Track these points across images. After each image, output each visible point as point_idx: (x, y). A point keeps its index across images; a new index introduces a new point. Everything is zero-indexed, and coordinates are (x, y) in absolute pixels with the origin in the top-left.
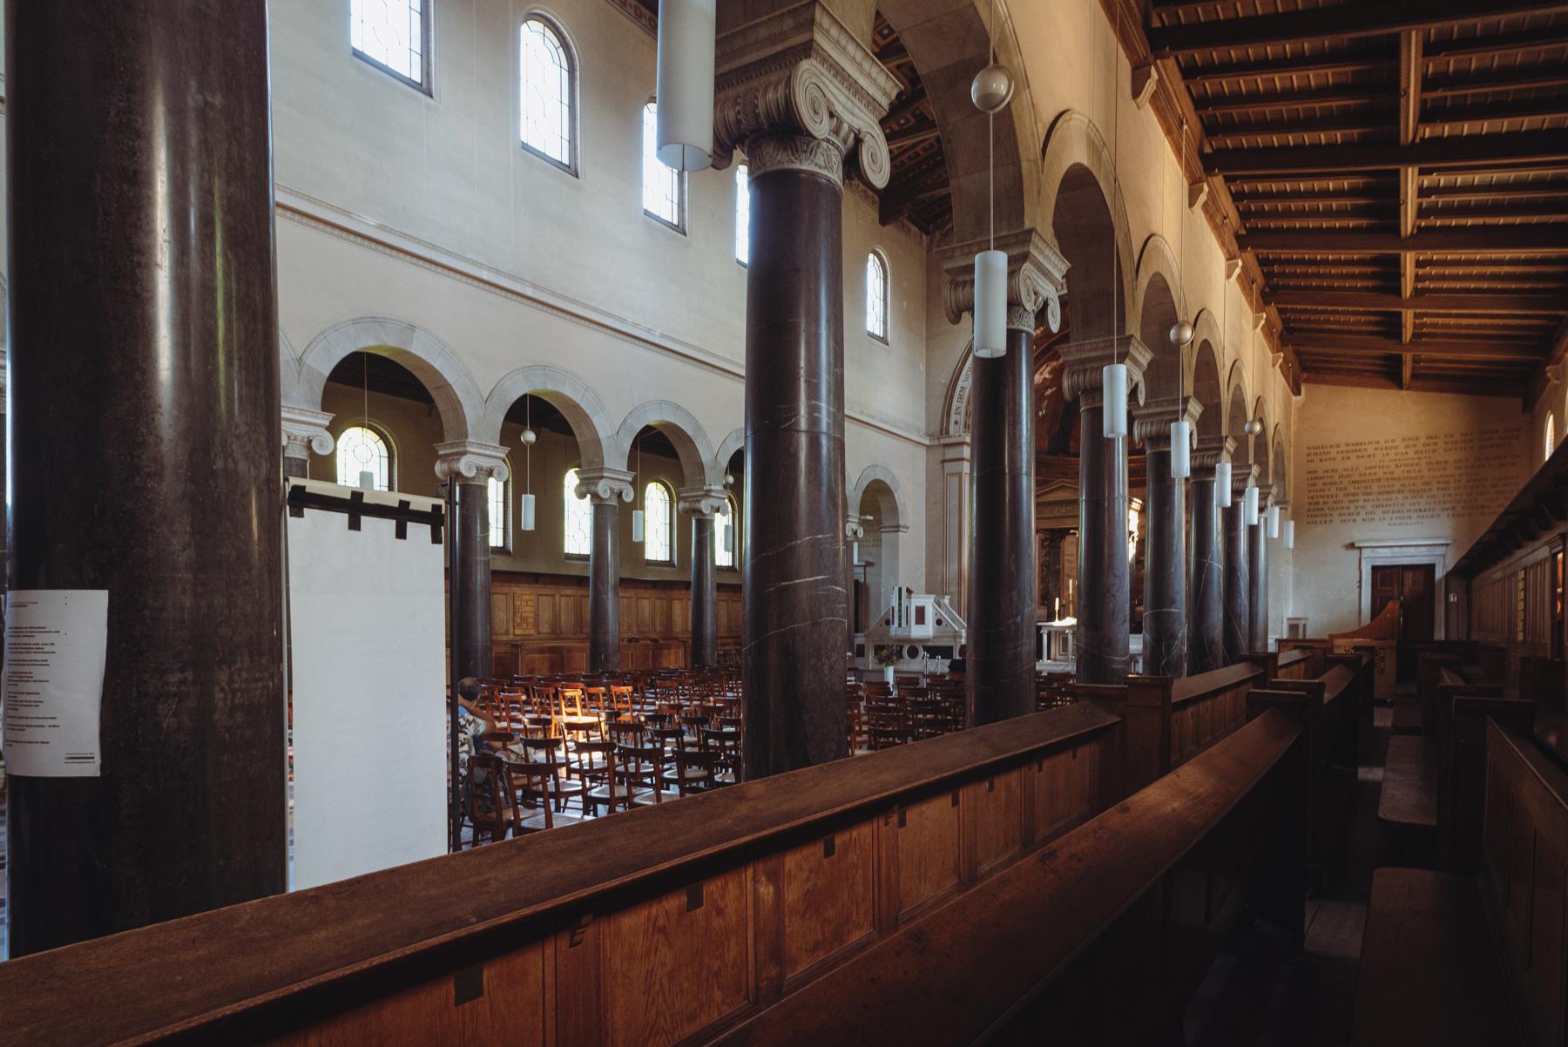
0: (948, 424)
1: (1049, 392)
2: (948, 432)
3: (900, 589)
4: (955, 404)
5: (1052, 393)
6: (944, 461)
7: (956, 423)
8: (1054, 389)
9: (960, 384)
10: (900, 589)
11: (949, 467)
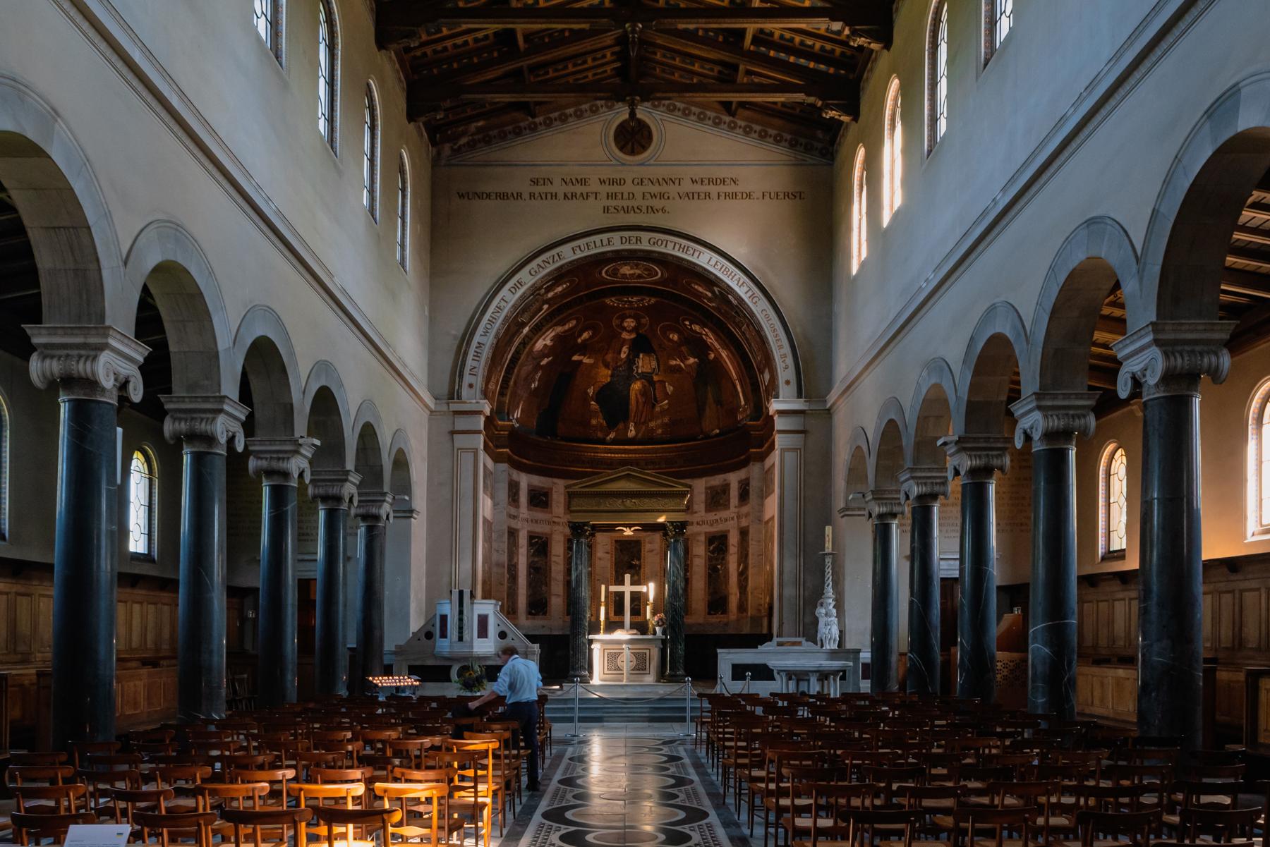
3: (461, 593)
5: (547, 363)
10: (461, 593)
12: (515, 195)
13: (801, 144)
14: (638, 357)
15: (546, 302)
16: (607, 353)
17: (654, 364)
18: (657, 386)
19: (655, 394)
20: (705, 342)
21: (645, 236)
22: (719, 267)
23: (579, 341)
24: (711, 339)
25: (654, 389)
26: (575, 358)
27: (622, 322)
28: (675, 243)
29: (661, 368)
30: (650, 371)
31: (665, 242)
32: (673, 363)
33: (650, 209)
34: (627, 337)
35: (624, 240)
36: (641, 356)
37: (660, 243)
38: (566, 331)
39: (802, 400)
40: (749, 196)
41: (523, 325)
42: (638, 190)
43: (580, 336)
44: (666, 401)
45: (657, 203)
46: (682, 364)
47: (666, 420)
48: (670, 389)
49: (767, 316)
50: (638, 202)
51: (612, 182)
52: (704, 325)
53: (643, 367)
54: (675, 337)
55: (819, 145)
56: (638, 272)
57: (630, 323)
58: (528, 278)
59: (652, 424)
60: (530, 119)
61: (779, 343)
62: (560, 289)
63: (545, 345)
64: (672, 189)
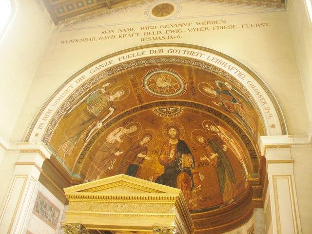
0: (29, 135)
1: (118, 153)
2: (27, 140)
4: (40, 121)
6: (17, 164)
7: (37, 135)
8: (122, 152)
9: (48, 107)
11: (20, 169)
12: (92, 39)
13: (264, 5)
14: (181, 157)
15: (111, 104)
16: (161, 155)
17: (191, 161)
18: (194, 176)
19: (193, 182)
20: (220, 138)
21: (165, 49)
22: (215, 60)
23: (142, 143)
24: (222, 133)
25: (192, 179)
26: (140, 155)
27: (168, 131)
28: (185, 51)
29: (196, 164)
30: (189, 166)
31: (178, 51)
32: (203, 159)
33: (170, 37)
34: (173, 143)
35: (152, 52)
36: (183, 156)
37: (175, 51)
38: (130, 134)
39: (287, 136)
40: (233, 27)
41: (93, 118)
42: (163, 30)
43: (142, 139)
44: (200, 185)
45: (175, 34)
46: (208, 159)
47: (200, 198)
48: (202, 177)
49: (253, 86)
50: (164, 34)
51: (148, 28)
52: (217, 123)
53: (184, 163)
54: (201, 140)
55: (276, 4)
56: (169, 84)
57: (173, 132)
58: (87, 75)
59: (191, 201)
60: (108, 10)
61: (263, 101)
62: (118, 94)
63: (116, 141)
64: (185, 28)
